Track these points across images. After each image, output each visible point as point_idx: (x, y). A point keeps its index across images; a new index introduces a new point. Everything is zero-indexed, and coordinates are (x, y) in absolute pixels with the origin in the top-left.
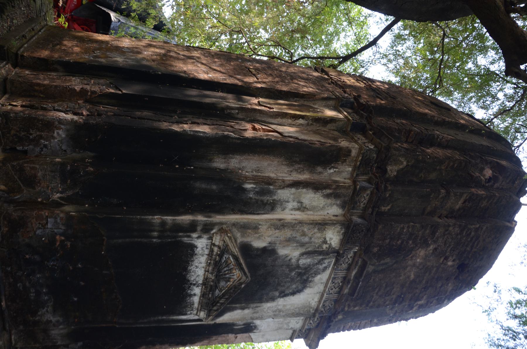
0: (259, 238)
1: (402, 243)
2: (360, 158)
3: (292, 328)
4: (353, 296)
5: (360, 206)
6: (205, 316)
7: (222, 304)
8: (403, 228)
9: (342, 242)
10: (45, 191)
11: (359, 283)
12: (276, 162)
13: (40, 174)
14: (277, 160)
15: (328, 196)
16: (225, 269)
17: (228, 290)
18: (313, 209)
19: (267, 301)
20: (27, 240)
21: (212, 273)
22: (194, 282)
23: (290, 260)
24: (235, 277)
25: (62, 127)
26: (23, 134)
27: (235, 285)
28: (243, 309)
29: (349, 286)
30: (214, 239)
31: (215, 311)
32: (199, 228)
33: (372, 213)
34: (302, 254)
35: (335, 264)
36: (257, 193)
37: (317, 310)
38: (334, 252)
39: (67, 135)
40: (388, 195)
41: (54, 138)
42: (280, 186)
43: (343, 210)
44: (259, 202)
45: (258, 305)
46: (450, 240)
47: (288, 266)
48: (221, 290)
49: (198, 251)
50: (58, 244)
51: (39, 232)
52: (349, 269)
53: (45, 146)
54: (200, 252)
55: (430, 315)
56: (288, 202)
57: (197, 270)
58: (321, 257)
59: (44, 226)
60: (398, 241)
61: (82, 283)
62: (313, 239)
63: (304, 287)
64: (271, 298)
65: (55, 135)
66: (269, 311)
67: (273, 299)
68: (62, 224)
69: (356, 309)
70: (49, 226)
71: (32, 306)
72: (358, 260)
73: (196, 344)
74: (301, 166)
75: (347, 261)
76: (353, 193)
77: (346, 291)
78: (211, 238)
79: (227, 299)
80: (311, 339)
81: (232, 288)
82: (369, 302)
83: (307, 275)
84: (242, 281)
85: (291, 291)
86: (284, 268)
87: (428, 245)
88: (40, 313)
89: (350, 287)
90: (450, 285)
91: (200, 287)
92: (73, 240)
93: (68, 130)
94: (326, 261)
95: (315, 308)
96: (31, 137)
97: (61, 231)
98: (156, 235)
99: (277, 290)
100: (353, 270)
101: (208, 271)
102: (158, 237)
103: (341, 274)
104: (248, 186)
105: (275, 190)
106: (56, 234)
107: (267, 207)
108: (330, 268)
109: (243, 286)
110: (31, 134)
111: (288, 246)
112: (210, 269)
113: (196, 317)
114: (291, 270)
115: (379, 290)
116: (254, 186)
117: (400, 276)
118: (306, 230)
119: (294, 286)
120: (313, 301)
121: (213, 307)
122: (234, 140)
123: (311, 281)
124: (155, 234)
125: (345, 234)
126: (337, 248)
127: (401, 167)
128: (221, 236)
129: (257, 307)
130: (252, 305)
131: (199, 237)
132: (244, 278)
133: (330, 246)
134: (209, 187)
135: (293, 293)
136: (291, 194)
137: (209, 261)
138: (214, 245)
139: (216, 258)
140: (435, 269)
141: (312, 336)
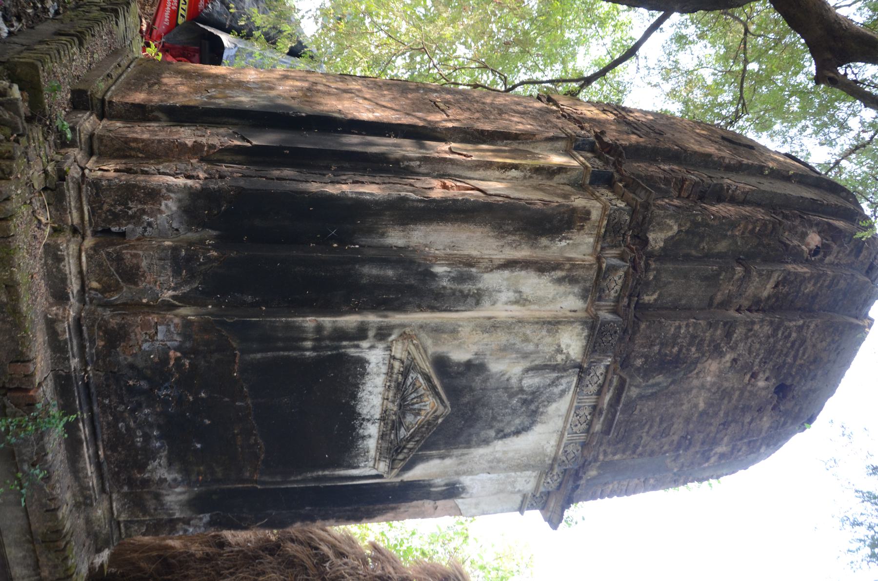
0: (459, 346)
1: (680, 351)
2: (605, 222)
3: (519, 491)
5: (609, 295)
6: (387, 469)
7: (410, 449)
8: (680, 327)
10: (151, 288)
12: (478, 234)
13: (144, 264)
14: (480, 230)
15: (560, 281)
16: (413, 396)
17: (419, 428)
18: (538, 301)
19: (478, 445)
20: (130, 359)
21: (393, 402)
22: (368, 417)
23: (508, 380)
24: (428, 408)
25: (172, 195)
26: (119, 208)
27: (428, 421)
28: (442, 457)
29: (602, 419)
30: (393, 350)
31: (401, 460)
32: (371, 334)
33: (629, 305)
34: (527, 370)
35: (577, 386)
36: (454, 279)
37: (555, 459)
38: (575, 367)
39: (179, 208)
40: (651, 277)
41: (160, 212)
42: (486, 268)
43: (585, 302)
44: (457, 293)
45: (465, 451)
46: (758, 346)
47: (506, 389)
48: (408, 429)
49: (371, 368)
50: (172, 363)
51: (145, 346)
52: (599, 393)
53: (150, 224)
54: (375, 370)
55: (741, 473)
56: (500, 292)
57: (371, 397)
58: (555, 375)
59: (152, 338)
60: (673, 347)
61: (207, 422)
62: (540, 347)
63: (533, 423)
64: (484, 441)
65: (163, 207)
67: (486, 442)
68: (178, 334)
69: (617, 457)
70: (160, 336)
71: (139, 457)
73: (376, 519)
74: (517, 238)
76: (598, 276)
77: (598, 427)
78: (389, 348)
79: (417, 441)
80: (551, 509)
81: (423, 425)
82: (636, 446)
83: (536, 404)
84: (438, 413)
85: (513, 429)
86: (500, 392)
87: (721, 355)
88: (149, 467)
89: (604, 421)
90: (765, 419)
91: (377, 425)
92: (192, 356)
93: (180, 201)
94: (564, 381)
95: (553, 455)
96: (130, 212)
97: (176, 344)
98: (310, 346)
99: (492, 427)
101: (387, 399)
102: (314, 349)
103: (590, 401)
104: (439, 269)
105: (479, 275)
106: (169, 348)
107: (469, 300)
108: (571, 392)
109: (440, 421)
110: (130, 208)
111: (503, 358)
112: (391, 394)
113: (374, 472)
114: (511, 396)
115: (651, 426)
116: (449, 269)
117: (682, 404)
118: (528, 332)
119: (517, 421)
120: (548, 445)
121: (398, 454)
122: (415, 204)
123: (542, 413)
124: (309, 344)
125: (589, 338)
126: (579, 361)
127: (670, 234)
128: (403, 343)
129: (463, 455)
130: (456, 452)
131: (372, 347)
132: (441, 408)
133: (567, 358)
134: (382, 273)
135: (517, 433)
136: (504, 279)
137: (388, 384)
138: (394, 358)
139: (397, 379)
140: (737, 393)
141: (552, 505)
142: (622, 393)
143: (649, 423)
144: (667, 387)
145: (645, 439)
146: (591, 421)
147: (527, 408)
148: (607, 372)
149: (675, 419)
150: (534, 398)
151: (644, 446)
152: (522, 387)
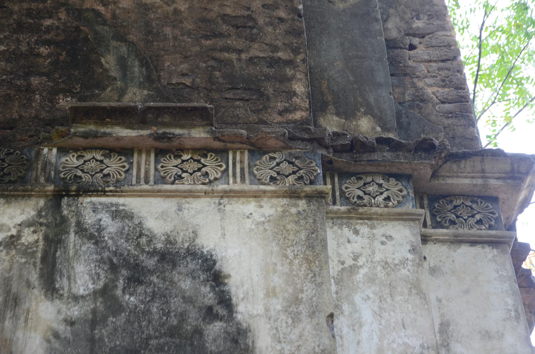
1: (48, 43)
3: (413, 250)
4: (205, 109)
9: (16, 197)
11: (150, 108)
29: (178, 131)
34: (51, 289)
35: (104, 193)
37: (293, 195)
38: (58, 206)
47: (95, 320)
52: (125, 151)
60: (39, 55)
63: (193, 253)
64: (235, 341)
66: (293, 337)
69: (299, 88)
72: (75, 134)
75: (93, 164)
77: (199, 134)
80: (480, 181)
82: (273, 62)
83: (142, 258)
85: (205, 289)
86: (99, 332)
89: (182, 127)
94: (89, 218)
95: (285, 201)
99: (198, 332)
100: (118, 139)
103: (146, 163)
108: (121, 200)
114: (115, 307)
115: (227, 49)
117: (176, 12)
119: (186, 284)
123: (169, 241)
126: (42, 202)
135: (217, 278)
141: (467, 181)
142: (104, 108)
143: (218, 55)
144: (131, 44)
145: (256, 51)
146: (195, 150)
147: (151, 272)
148: (76, 150)
149: (212, 15)
150: (126, 264)
151: (276, 49)
152: (95, 294)
